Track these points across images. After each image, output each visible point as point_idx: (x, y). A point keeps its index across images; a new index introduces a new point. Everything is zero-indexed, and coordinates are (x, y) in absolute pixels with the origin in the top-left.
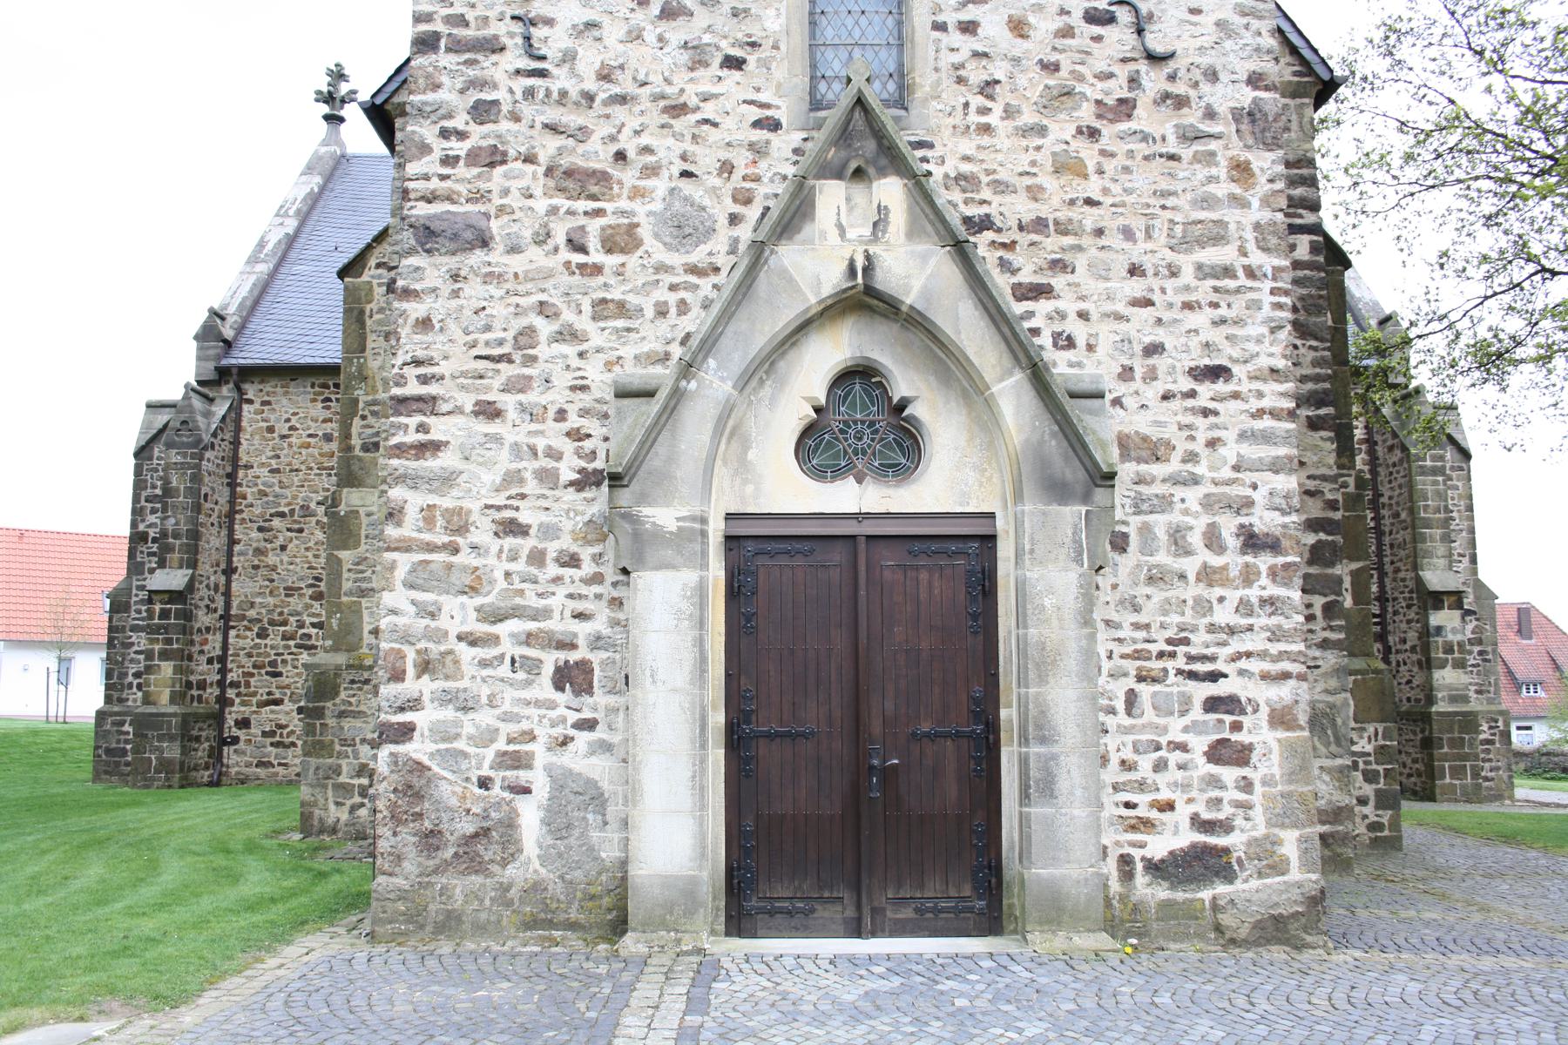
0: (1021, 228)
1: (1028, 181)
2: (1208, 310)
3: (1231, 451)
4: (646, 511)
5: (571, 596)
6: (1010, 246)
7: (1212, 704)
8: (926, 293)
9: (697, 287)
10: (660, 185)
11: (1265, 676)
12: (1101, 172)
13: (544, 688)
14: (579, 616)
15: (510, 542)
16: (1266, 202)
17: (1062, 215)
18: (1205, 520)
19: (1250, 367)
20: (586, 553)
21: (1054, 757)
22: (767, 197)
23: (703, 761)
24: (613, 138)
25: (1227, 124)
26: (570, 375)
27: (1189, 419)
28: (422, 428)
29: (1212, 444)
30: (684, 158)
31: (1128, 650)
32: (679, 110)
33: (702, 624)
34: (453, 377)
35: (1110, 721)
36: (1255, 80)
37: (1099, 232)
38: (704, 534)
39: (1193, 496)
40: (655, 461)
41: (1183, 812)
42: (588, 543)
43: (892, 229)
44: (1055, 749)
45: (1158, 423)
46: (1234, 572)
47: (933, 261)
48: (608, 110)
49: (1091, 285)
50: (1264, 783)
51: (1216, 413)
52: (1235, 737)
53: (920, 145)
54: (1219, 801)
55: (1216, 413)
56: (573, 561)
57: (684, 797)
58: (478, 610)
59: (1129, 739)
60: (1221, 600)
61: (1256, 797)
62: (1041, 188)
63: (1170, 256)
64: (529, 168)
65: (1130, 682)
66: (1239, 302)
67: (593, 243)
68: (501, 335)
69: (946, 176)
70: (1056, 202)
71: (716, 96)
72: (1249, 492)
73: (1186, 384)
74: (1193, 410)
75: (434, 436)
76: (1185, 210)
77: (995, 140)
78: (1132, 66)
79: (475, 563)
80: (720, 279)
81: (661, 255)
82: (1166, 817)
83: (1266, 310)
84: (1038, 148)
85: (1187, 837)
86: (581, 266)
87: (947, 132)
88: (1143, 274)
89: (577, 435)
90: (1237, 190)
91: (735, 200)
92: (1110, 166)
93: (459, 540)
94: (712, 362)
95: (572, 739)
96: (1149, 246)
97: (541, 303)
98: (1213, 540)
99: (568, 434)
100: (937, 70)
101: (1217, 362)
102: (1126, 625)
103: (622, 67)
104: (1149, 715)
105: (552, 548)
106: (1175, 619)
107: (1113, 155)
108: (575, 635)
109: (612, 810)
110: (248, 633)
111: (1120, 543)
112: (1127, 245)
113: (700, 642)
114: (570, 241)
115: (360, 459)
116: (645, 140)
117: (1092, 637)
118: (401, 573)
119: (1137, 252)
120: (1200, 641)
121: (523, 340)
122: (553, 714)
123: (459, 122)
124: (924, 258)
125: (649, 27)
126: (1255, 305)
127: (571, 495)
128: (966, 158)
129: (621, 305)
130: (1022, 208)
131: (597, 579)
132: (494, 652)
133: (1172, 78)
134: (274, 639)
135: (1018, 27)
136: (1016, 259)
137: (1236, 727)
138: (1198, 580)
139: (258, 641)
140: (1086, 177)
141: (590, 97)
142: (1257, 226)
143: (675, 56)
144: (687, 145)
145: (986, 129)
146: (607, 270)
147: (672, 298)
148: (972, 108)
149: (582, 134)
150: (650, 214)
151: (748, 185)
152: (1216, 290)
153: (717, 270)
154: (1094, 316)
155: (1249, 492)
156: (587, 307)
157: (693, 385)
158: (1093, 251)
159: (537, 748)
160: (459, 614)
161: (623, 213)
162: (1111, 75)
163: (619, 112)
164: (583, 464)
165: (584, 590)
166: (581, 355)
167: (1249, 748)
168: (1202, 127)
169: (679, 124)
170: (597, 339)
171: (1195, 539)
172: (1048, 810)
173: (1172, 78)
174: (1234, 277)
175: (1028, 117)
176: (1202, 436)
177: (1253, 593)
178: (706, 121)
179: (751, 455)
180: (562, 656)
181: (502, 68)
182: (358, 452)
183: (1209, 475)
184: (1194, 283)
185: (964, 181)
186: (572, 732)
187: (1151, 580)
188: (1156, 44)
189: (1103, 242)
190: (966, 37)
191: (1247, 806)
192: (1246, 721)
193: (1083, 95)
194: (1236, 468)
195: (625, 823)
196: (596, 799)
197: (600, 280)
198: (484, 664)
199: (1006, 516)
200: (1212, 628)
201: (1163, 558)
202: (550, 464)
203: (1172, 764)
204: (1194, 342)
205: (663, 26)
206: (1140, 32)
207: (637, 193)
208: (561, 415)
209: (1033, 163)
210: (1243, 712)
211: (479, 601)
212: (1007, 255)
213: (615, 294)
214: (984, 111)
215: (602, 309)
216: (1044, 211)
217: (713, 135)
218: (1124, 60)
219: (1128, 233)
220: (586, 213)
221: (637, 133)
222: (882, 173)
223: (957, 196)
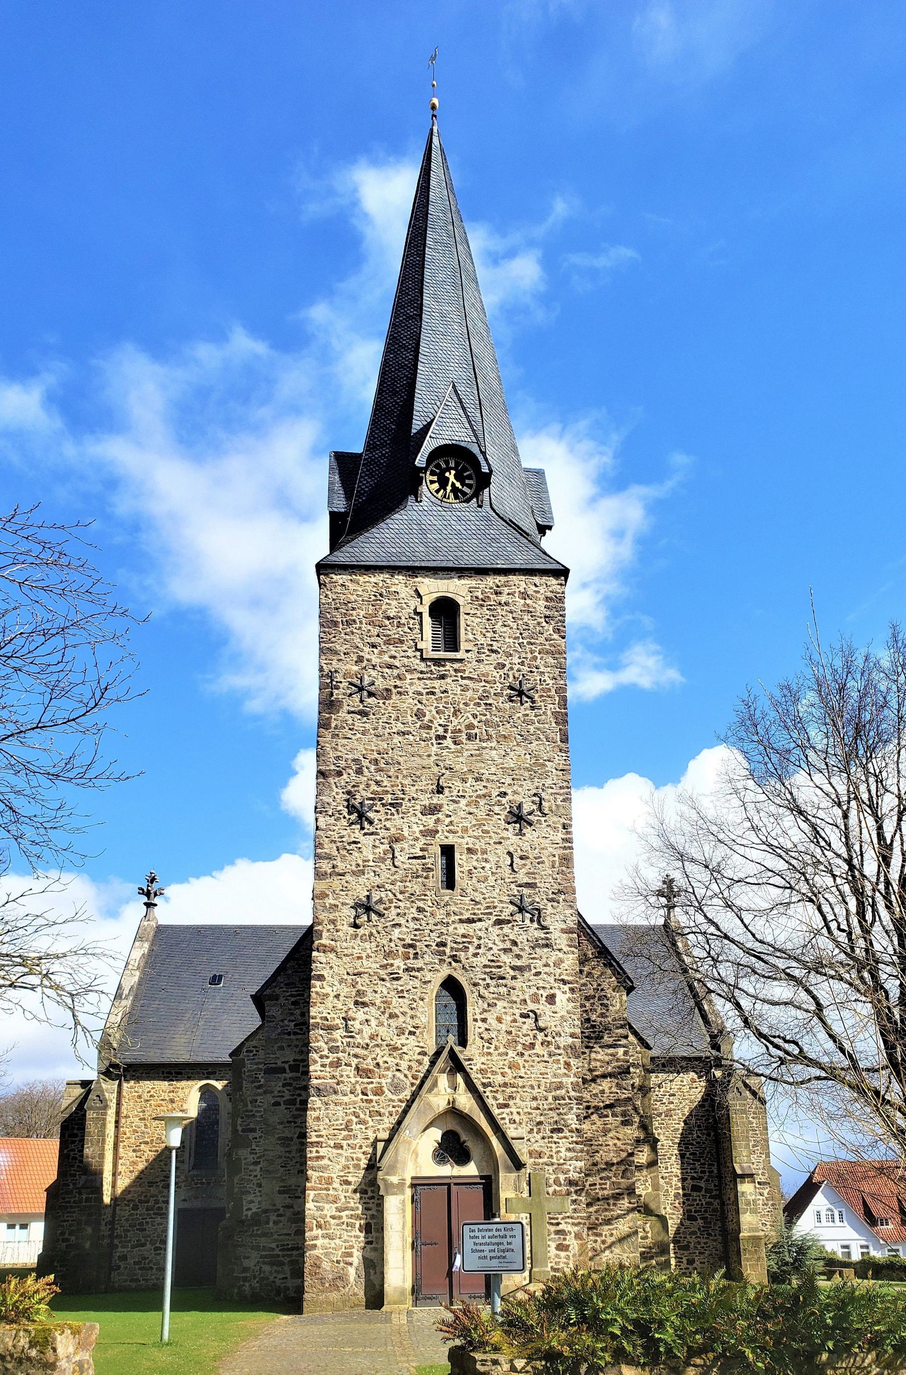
1: (502, 1070)
3: (562, 1155)
6: (497, 1092)
10: (390, 1074)
11: (573, 1224)
15: (345, 1187)
16: (575, 1075)
17: (512, 1082)
20: (369, 1190)
28: (317, 1152)
30: (397, 1065)
32: (396, 1049)
33: (404, 1211)
36: (572, 1035)
42: (370, 1187)
45: (541, 1146)
46: (564, 1192)
53: (469, 1060)
64: (349, 1068)
67: (369, 1093)
75: (321, 1154)
81: (390, 1096)
86: (366, 1100)
116: (385, 1059)
118: (311, 1198)
119: (535, 1092)
123: (326, 1052)
126: (572, 1108)
128: (483, 1063)
133: (546, 1036)
134: (142, 1210)
135: (499, 1020)
136: (499, 1096)
137: (565, 1239)
142: (572, 1083)
144: (398, 1061)
145: (490, 1054)
160: (329, 1210)
163: (378, 1050)
166: (366, 1128)
167: (569, 1246)
170: (371, 1123)
171: (551, 1181)
173: (546, 1036)
175: (502, 1050)
176: (554, 1150)
181: (338, 1034)
188: (541, 1024)
192: (568, 1237)
198: (338, 1225)
205: (391, 1021)
208: (361, 1147)
211: (336, 1205)
214: (488, 1048)
217: (406, 1057)
219: (532, 1087)
223: (480, 1076)
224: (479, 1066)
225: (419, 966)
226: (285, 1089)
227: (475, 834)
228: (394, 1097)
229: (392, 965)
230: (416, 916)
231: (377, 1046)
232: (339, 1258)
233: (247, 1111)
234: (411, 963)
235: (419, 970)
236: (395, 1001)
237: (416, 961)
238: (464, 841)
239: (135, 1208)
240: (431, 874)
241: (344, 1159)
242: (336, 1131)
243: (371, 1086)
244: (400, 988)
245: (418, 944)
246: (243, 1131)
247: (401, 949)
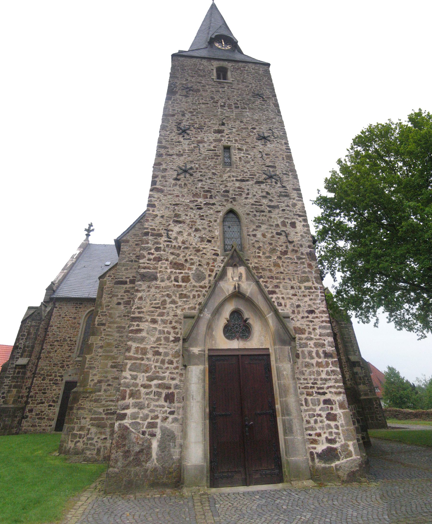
1: (269, 268)
2: (308, 297)
6: (266, 282)
8: (251, 293)
9: (202, 291)
10: (194, 267)
19: (319, 310)
22: (216, 271)
34: (147, 312)
37: (284, 279)
43: (243, 278)
47: (252, 285)
49: (284, 291)
58: (147, 377)
62: (271, 270)
66: (314, 295)
67: (180, 280)
68: (158, 302)
69: (252, 267)
70: (275, 272)
79: (147, 363)
80: (207, 289)
86: (177, 285)
88: (294, 288)
91: (210, 271)
93: (144, 356)
96: (294, 282)
97: (168, 294)
110: (40, 379)
112: (290, 282)
114: (175, 279)
115: (96, 328)
121: (163, 303)
122: (164, 409)
124: (250, 285)
129: (185, 295)
130: (268, 274)
132: (150, 390)
139: (42, 381)
146: (183, 287)
150: (192, 274)
151: (212, 268)
153: (206, 287)
156: (178, 295)
158: (283, 283)
161: (186, 273)
174: (312, 289)
182: (96, 326)
184: (305, 291)
185: (256, 268)
186: (168, 415)
189: (285, 281)
197: (181, 289)
207: (189, 269)
212: (266, 284)
213: (184, 292)
216: (272, 275)
217: (206, 257)
219: (290, 279)
220: (178, 273)
224: (253, 265)
225: (213, 202)
226: (125, 294)
227: (241, 142)
228: (197, 284)
229: (197, 201)
230: (211, 177)
231: (187, 248)
232: (144, 429)
233: (102, 312)
234: (208, 200)
235: (214, 204)
236: (199, 222)
237: (211, 200)
238: (237, 145)
239: (43, 380)
240: (219, 158)
241: (157, 333)
242: (153, 309)
243: (182, 275)
244: (202, 214)
245: (212, 190)
246: (98, 325)
247: (203, 193)
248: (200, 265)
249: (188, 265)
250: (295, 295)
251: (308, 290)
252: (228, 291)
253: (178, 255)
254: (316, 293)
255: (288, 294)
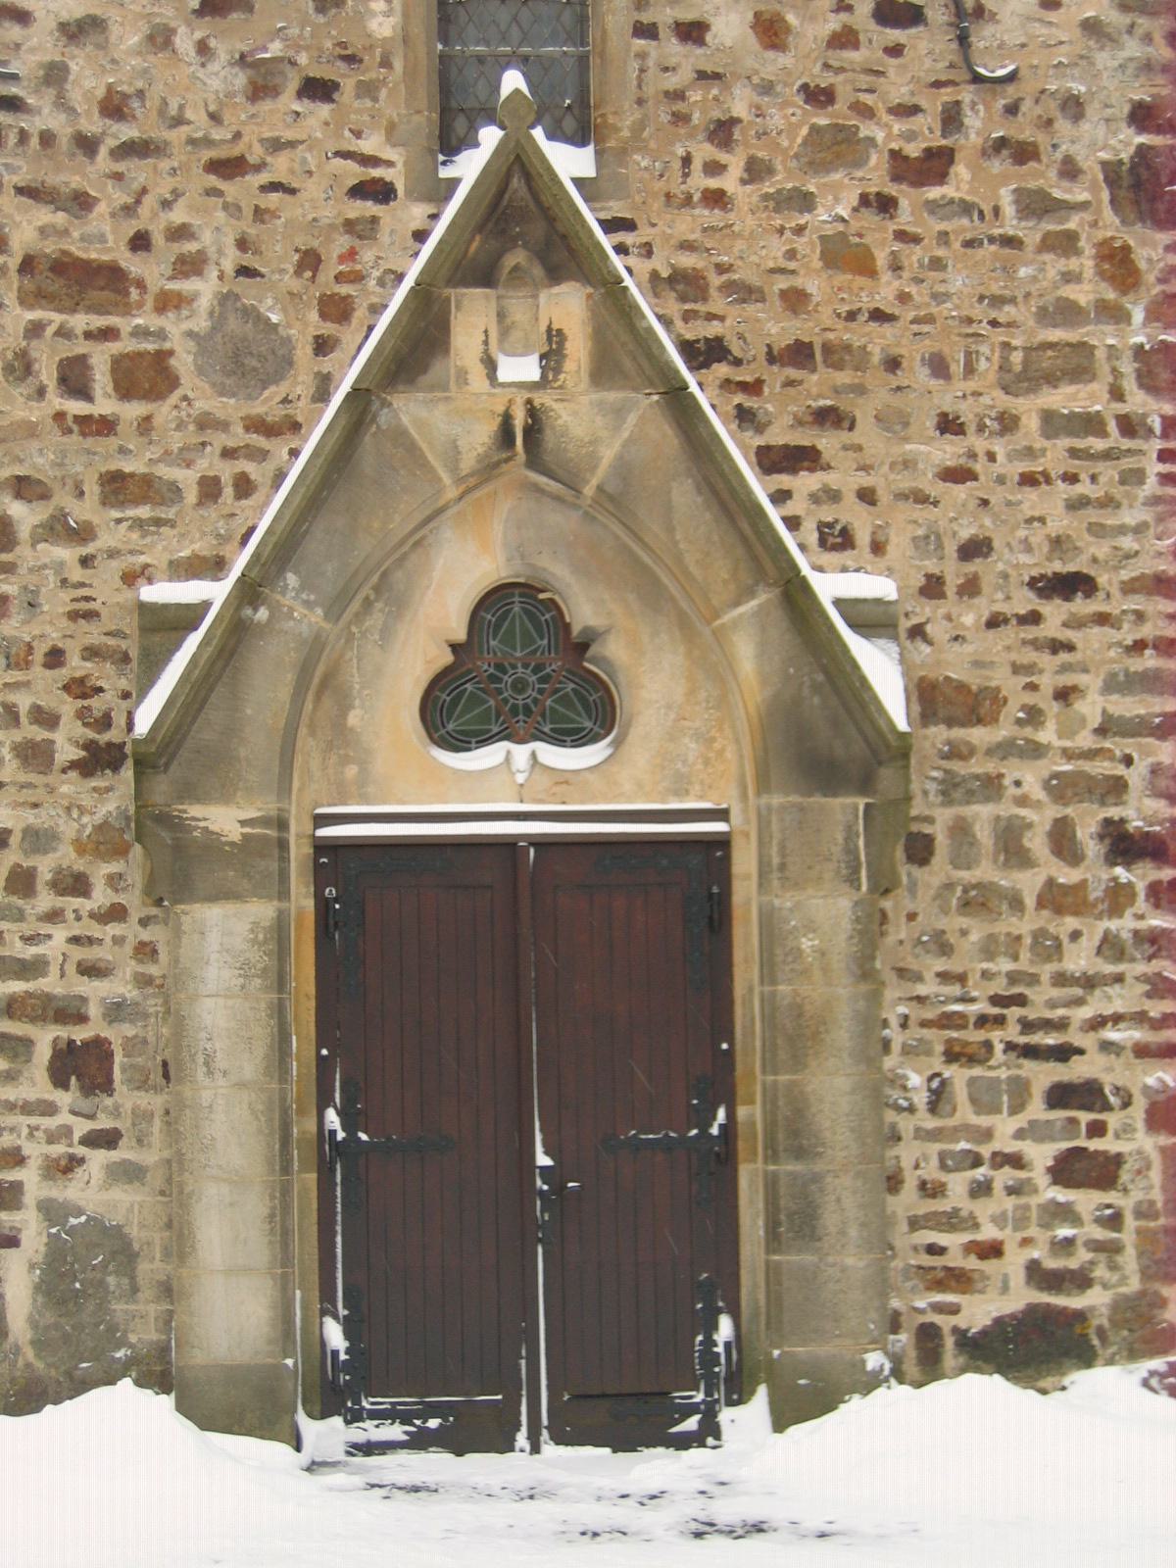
0: (771, 358)
1: (782, 283)
2: (1061, 485)
3: (1091, 707)
4: (195, 811)
5: (75, 940)
6: (754, 388)
7: (1061, 1096)
10: (205, 289)
11: (1142, 1051)
12: (896, 267)
13: (36, 1084)
14: (90, 970)
18: (1053, 812)
21: (817, 1178)
23: (286, 1191)
24: (129, 210)
25: (1094, 188)
26: (66, 596)
27: (1029, 656)
29: (1064, 695)
30: (242, 244)
31: (930, 1014)
32: (230, 167)
35: (906, 1124)
38: (283, 845)
39: (1030, 777)
40: (205, 733)
41: (1015, 1261)
43: (569, 366)
44: (819, 1166)
46: (1095, 893)
48: (120, 167)
50: (1139, 1214)
51: (1070, 647)
52: (1095, 1145)
54: (1069, 1243)
55: (1070, 647)
56: (78, 885)
57: (258, 1248)
59: (936, 1147)
60: (1075, 936)
61: (1128, 1236)
63: (1004, 401)
65: (937, 1064)
67: (101, 379)
71: (292, 144)
72: (1120, 770)
73: (1024, 601)
74: (1036, 644)
76: (1028, 331)
77: (732, 217)
78: (946, 95)
82: (989, 1266)
83: (1151, 486)
84: (800, 230)
85: (1020, 1297)
86: (83, 421)
87: (658, 204)
89: (80, 688)
90: (1111, 295)
92: (914, 255)
94: (292, 579)
95: (81, 1161)
96: (972, 385)
97: (19, 479)
98: (1063, 842)
99: (66, 688)
100: (640, 102)
101: (1071, 568)
102: (929, 976)
103: (140, 94)
104: (965, 1113)
105: (45, 867)
106: (1005, 965)
107: (916, 239)
108: (84, 1000)
109: (150, 1268)
111: (920, 850)
113: (279, 1011)
114: (63, 380)
116: (178, 216)
117: (875, 998)
119: (947, 397)
120: (1042, 999)
124: (619, 413)
125: (182, 30)
126: (1137, 476)
127: (70, 786)
128: (687, 246)
129: (147, 481)
131: (117, 913)
136: (765, 405)
137: (1097, 1130)
138: (1041, 904)
140: (871, 272)
141: (87, 145)
143: (221, 78)
145: (716, 199)
147: (226, 471)
148: (697, 165)
149: (82, 202)
150: (190, 334)
151: (344, 289)
152: (1074, 453)
154: (884, 497)
155: (1120, 770)
156: (92, 489)
157: (263, 614)
159: (29, 1176)
161: (140, 333)
162: (914, 110)
163: (139, 171)
164: (91, 734)
165: (96, 930)
166: (86, 562)
168: (1057, 194)
169: (231, 189)
171: (1037, 843)
172: (809, 1258)
174: (1103, 433)
175: (782, 180)
176: (1048, 682)
177: (1124, 925)
178: (274, 187)
179: (353, 719)
180: (63, 1032)
183: (1057, 743)
186: (81, 1151)
187: (966, 905)
189: (901, 378)
190: (690, 47)
191: (1111, 1249)
192: (1113, 1120)
193: (871, 141)
194: (1102, 731)
195: (167, 1290)
196: (122, 1251)
197: (113, 442)
199: (745, 811)
200: (1061, 979)
201: (985, 871)
202: (39, 734)
203: (998, 1186)
204: (1038, 536)
206: (963, 40)
207: (167, 302)
208: (55, 658)
209: (791, 254)
210: (1107, 1107)
212: (750, 402)
214: (714, 168)
215: (117, 487)
218: (937, 84)
219: (939, 366)
220: (88, 335)
221: (166, 204)
222: (555, 275)
243: (115, 347)
248: (244, 271)
249: (152, 271)
250: (957, 475)
251: (1065, 442)
252: (453, 453)
253: (82, 202)
254: (1127, 463)
255: (907, 464)
